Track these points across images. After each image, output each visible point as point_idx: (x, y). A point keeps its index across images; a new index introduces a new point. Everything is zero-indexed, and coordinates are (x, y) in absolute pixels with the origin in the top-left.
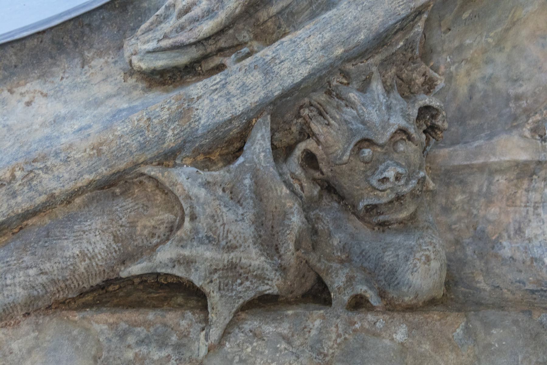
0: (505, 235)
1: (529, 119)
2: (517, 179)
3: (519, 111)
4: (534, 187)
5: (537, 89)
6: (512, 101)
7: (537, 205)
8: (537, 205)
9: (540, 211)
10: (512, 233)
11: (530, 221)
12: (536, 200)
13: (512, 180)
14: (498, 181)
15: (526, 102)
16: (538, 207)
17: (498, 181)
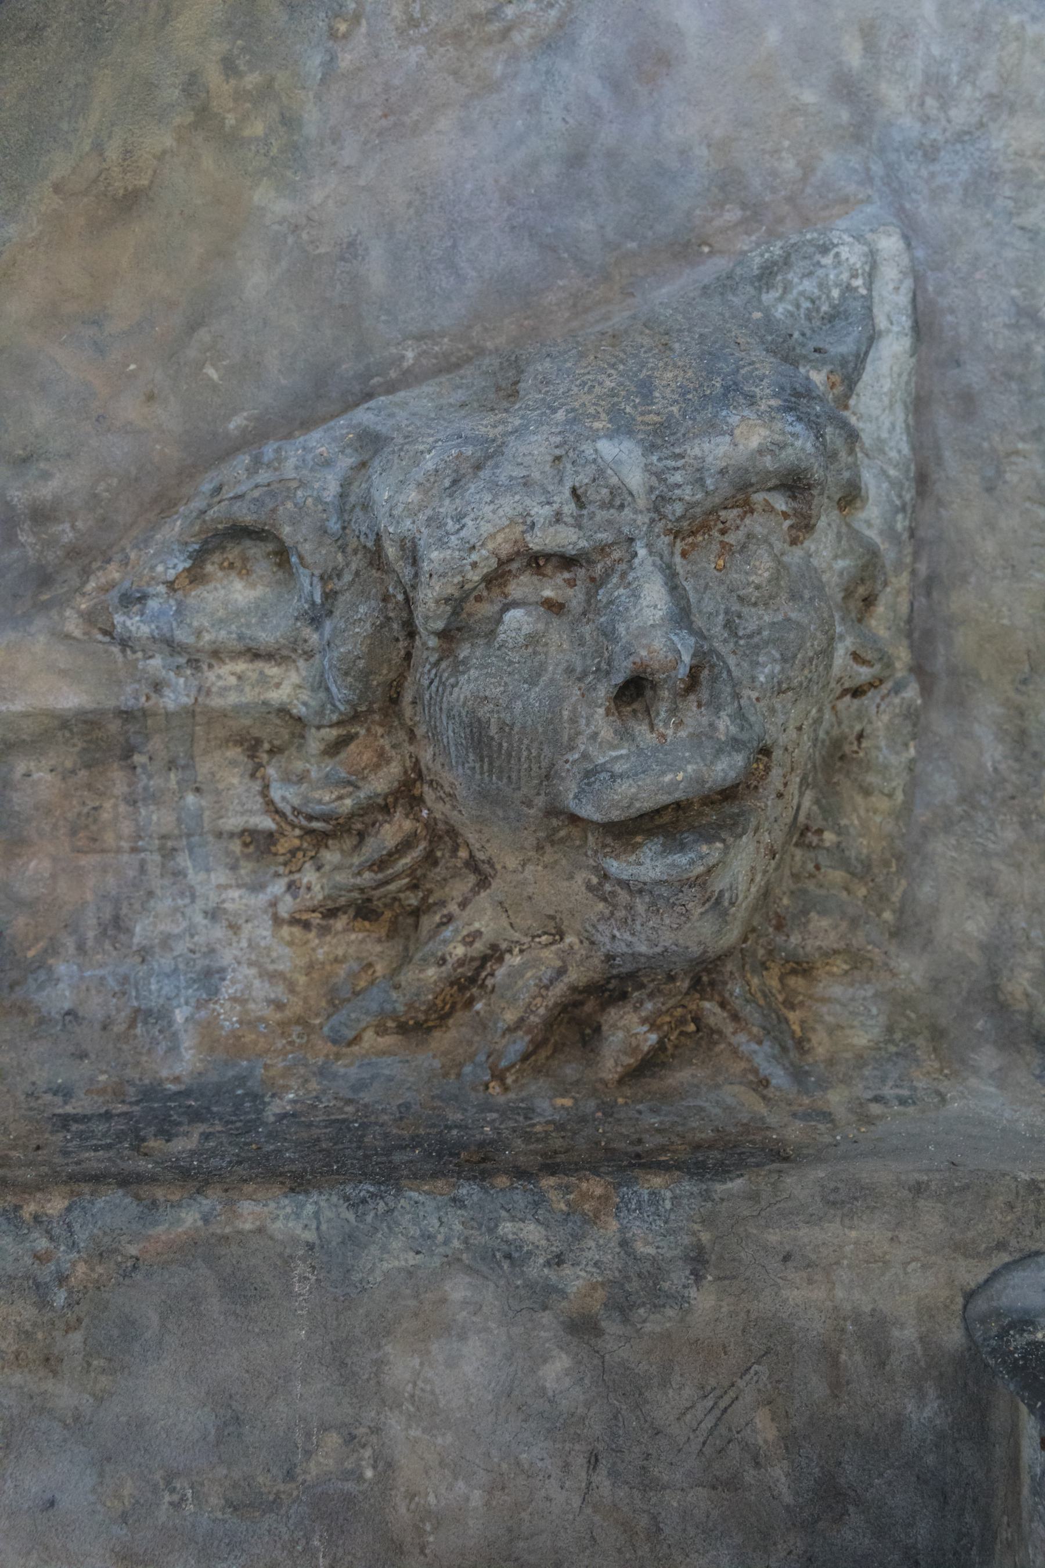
0: (70, 943)
1: (87, 581)
2: (88, 767)
3: (51, 557)
4: (146, 788)
5: (101, 487)
6: (26, 527)
7: (170, 844)
8: (170, 844)
9: (183, 860)
10: (91, 934)
11: (150, 894)
12: (164, 830)
13: (73, 772)
14: (28, 775)
15: (73, 527)
16: (174, 849)
17: (28, 775)
